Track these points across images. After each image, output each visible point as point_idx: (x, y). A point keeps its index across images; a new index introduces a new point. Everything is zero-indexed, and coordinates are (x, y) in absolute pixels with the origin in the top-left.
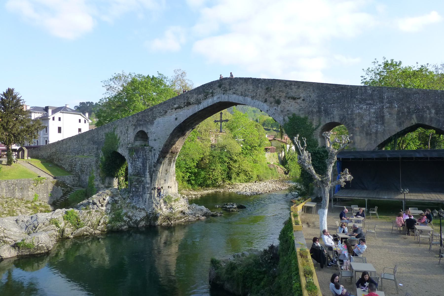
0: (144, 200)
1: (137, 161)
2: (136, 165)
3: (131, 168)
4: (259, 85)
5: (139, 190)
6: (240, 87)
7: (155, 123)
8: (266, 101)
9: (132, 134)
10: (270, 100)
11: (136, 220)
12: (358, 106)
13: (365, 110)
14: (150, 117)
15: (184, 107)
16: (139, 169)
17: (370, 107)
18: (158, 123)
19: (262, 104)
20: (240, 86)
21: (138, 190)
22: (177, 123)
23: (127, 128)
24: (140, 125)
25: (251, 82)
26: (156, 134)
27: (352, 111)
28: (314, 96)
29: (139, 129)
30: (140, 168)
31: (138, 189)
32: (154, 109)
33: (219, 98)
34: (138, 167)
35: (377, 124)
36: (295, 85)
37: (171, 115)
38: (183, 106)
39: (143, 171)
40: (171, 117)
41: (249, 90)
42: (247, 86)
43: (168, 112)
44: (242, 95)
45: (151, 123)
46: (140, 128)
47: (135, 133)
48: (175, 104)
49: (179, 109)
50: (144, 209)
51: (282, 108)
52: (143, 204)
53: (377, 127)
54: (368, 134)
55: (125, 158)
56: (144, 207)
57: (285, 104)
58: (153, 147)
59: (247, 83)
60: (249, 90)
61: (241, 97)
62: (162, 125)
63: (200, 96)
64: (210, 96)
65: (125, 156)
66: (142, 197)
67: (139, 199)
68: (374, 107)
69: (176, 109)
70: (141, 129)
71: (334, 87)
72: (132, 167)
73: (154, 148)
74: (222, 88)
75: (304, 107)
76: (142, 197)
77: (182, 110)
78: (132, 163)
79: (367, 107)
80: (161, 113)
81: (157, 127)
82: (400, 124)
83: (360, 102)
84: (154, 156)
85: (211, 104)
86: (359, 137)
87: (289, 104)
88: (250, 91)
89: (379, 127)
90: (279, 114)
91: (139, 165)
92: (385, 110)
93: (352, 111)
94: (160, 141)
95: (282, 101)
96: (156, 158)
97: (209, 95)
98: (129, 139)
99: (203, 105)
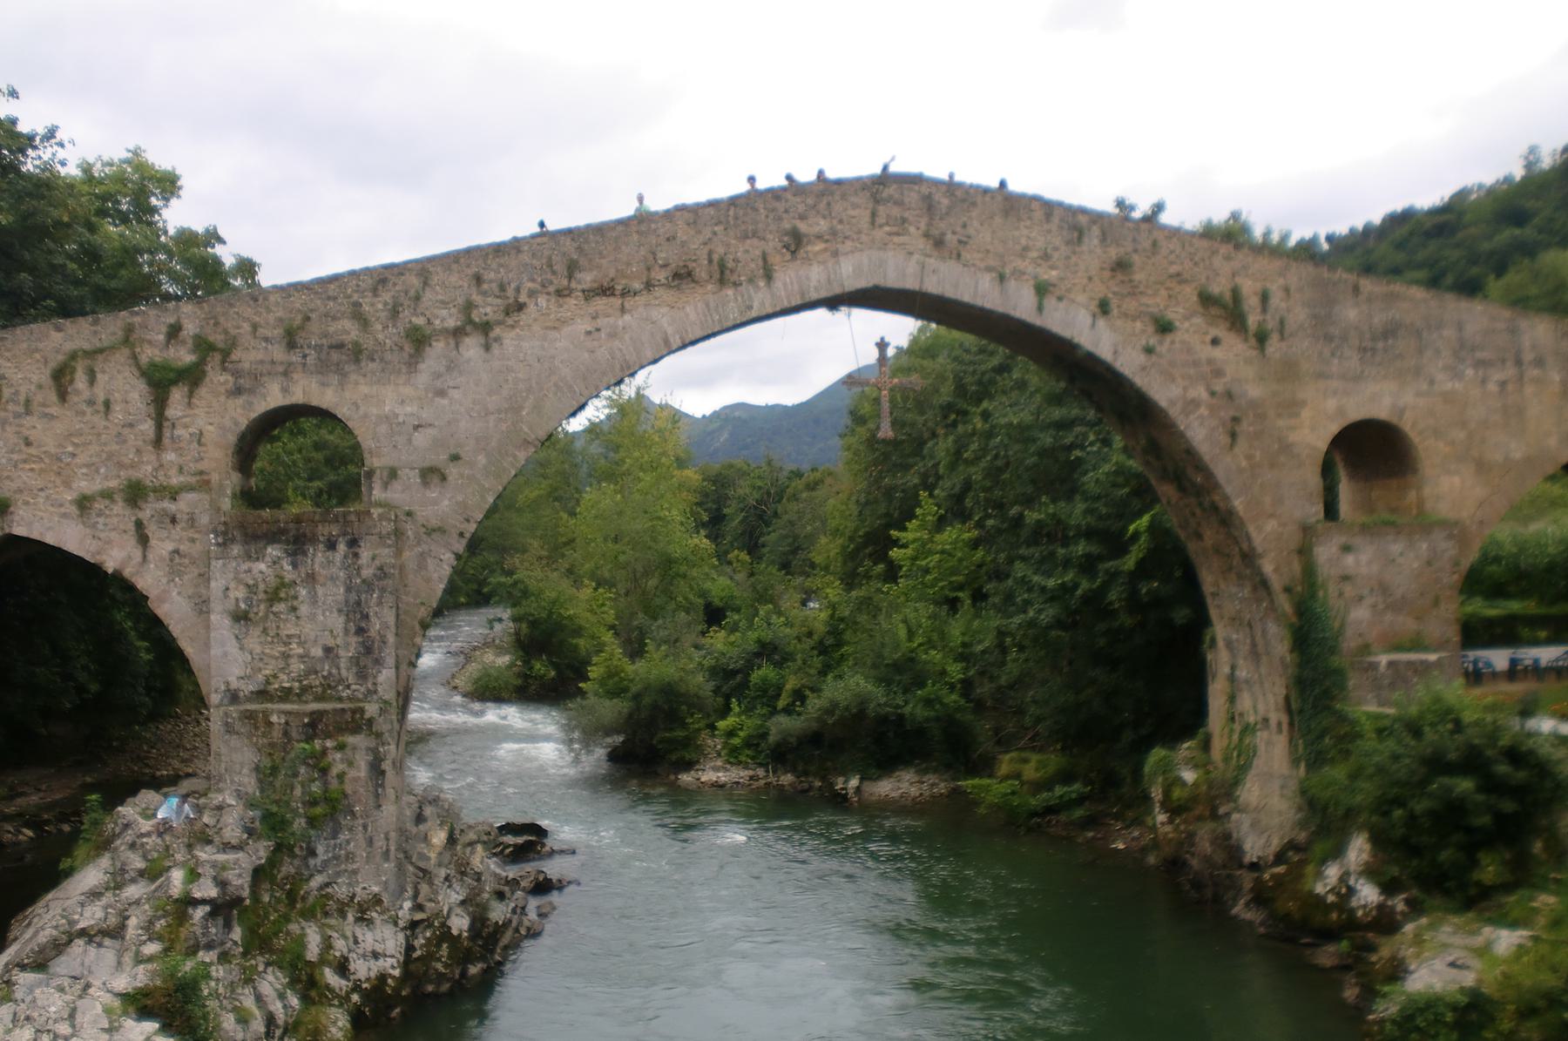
2: (292, 632)
7: (422, 366)
10: (1125, 306)
11: (382, 977)
15: (649, 286)
16: (317, 652)
18: (449, 369)
25: (1039, 214)
26: (430, 431)
27: (1432, 382)
29: (274, 397)
30: (328, 650)
37: (555, 328)
38: (637, 285)
39: (355, 661)
40: (553, 334)
41: (1026, 249)
42: (1017, 228)
43: (531, 307)
44: (989, 269)
45: (382, 360)
46: (285, 390)
47: (241, 414)
49: (616, 302)
50: (377, 900)
51: (1177, 345)
54: (1482, 467)
56: (376, 889)
57: (1187, 331)
60: (1026, 249)
63: (755, 241)
66: (365, 827)
67: (348, 842)
69: (589, 294)
70: (297, 397)
74: (887, 224)
76: (365, 827)
81: (441, 393)
84: (422, 566)
88: (1034, 254)
92: (1529, 390)
93: (1432, 382)
97: (809, 248)
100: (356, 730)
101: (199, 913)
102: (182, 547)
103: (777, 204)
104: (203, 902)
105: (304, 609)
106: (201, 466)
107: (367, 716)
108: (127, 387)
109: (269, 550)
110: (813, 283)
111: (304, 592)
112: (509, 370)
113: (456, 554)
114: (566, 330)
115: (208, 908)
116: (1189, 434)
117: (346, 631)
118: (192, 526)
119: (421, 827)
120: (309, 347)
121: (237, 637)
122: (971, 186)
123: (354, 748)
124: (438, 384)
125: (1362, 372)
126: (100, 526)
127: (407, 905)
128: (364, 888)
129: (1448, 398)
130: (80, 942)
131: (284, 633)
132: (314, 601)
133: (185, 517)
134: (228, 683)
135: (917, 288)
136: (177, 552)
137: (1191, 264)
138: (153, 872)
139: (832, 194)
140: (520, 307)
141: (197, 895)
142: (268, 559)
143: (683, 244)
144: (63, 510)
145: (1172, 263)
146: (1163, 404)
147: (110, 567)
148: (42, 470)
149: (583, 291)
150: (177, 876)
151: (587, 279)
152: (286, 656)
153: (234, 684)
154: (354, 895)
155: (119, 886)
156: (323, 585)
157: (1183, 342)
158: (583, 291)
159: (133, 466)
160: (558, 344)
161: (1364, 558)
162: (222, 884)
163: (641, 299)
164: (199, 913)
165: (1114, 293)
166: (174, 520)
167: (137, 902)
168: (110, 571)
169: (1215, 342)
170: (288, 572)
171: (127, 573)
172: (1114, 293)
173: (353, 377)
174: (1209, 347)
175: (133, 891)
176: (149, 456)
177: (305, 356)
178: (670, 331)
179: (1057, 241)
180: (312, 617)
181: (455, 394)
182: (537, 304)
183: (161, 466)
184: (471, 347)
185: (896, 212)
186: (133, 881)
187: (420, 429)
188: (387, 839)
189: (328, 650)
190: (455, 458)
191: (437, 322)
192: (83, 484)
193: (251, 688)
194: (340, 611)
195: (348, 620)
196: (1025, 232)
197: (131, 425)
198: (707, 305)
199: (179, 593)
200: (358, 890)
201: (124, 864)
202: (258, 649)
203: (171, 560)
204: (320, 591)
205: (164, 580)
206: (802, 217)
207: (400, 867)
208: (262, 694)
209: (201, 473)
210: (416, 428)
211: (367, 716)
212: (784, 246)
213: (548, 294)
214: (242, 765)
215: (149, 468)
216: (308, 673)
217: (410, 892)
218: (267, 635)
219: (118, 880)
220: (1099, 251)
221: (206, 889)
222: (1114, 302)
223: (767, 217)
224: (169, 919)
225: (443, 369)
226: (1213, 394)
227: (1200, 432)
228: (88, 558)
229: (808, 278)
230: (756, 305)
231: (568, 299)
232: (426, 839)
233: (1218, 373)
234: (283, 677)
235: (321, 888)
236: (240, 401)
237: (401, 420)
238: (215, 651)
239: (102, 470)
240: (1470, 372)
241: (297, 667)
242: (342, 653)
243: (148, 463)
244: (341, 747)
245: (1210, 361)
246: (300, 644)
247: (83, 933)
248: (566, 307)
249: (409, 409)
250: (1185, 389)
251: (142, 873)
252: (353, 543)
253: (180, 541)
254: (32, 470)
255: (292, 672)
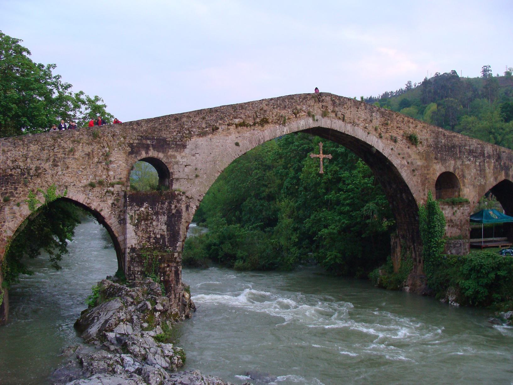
0: (177, 296)
1: (152, 219)
2: (151, 229)
3: (136, 234)
4: (374, 114)
5: (170, 279)
6: (348, 111)
7: (188, 146)
8: (381, 137)
9: (121, 162)
12: (467, 158)
13: (472, 161)
14: (175, 134)
15: (254, 124)
17: (475, 160)
18: (196, 147)
19: (376, 140)
20: (348, 110)
21: (169, 277)
22: (239, 151)
23: (107, 149)
24: (147, 148)
26: (190, 167)
28: (431, 141)
30: (161, 235)
31: (168, 276)
32: (184, 119)
33: (317, 120)
34: (156, 231)
35: (481, 177)
36: (412, 123)
37: (227, 136)
42: (357, 111)
43: (220, 130)
44: (350, 123)
45: (176, 144)
46: (147, 153)
48: (235, 118)
49: (245, 128)
50: (177, 314)
51: (399, 148)
52: (176, 305)
53: (480, 180)
55: (102, 213)
57: (401, 144)
58: (184, 193)
59: (358, 108)
60: (359, 117)
61: (349, 125)
62: (206, 151)
64: (303, 114)
65: (101, 210)
66: (174, 292)
68: (478, 161)
69: (237, 126)
71: (448, 134)
72: (140, 233)
73: (187, 195)
75: (421, 152)
76: (174, 292)
77: (250, 130)
78: (137, 225)
79: (473, 159)
80: (204, 128)
81: (194, 155)
82: (496, 178)
83: (469, 155)
85: (305, 128)
86: (468, 189)
87: (406, 145)
88: (362, 119)
89: (482, 180)
90: (397, 156)
91: (159, 228)
92: (486, 165)
94: (202, 183)
95: (398, 139)
96: (191, 214)
97: (300, 114)
98: (111, 173)
99: (290, 128)
100: (172, 261)
101: (157, 314)
102: (115, 202)
103: (292, 101)
104: (160, 311)
105: (154, 223)
106: (122, 176)
107: (175, 256)
108: (99, 150)
109: (145, 204)
110: (302, 125)
111: (155, 217)
112: (214, 149)
113: (197, 206)
114: (230, 137)
116: (402, 174)
117: (167, 231)
118: (118, 196)
120: (154, 139)
121: (135, 231)
122: (345, 98)
123: (172, 267)
124: (193, 152)
125: (446, 158)
126: (90, 195)
127: (184, 315)
128: (174, 310)
129: (468, 167)
130: (122, 323)
131: (148, 230)
132: (158, 221)
133: (117, 192)
134: (132, 246)
135: (329, 127)
136: (113, 204)
137: (403, 124)
139: (307, 98)
140: (218, 128)
141: (158, 309)
142: (144, 206)
143: (265, 111)
144: (79, 189)
145: (399, 124)
146: (395, 166)
147: (93, 207)
148: (72, 176)
149: (236, 124)
151: (237, 121)
152: (149, 238)
153: (134, 246)
155: (126, 307)
156: (161, 215)
157: (400, 147)
158: (236, 124)
159: (101, 176)
160: (228, 141)
161: (447, 212)
162: (164, 306)
163: (253, 128)
164: (157, 314)
165: (382, 132)
166: (113, 194)
168: (93, 209)
169: (409, 148)
170: (150, 211)
171: (98, 210)
172: (382, 132)
173: (167, 149)
174: (408, 149)
176: (105, 172)
177: (153, 142)
178: (260, 138)
179: (368, 116)
180: (157, 226)
181: (197, 155)
182: (222, 128)
183: (109, 176)
184: (202, 141)
185: (324, 104)
186: (130, 305)
187: (187, 166)
188: (180, 295)
189: (161, 235)
190: (197, 176)
191: (192, 133)
192: (85, 181)
193: (139, 247)
194: (166, 224)
195: (167, 227)
196: (359, 112)
197: (101, 162)
198: (271, 131)
199: (114, 217)
201: (127, 300)
202: (141, 236)
203: (112, 206)
204: (160, 217)
205: (110, 213)
206: (299, 105)
208: (143, 248)
209: (120, 179)
210: (186, 166)
211: (175, 256)
212: (293, 113)
213: (225, 125)
214: (138, 271)
215: (105, 177)
216: (156, 243)
218: (144, 231)
220: (379, 119)
222: (383, 135)
223: (289, 104)
224: (149, 316)
225: (194, 148)
226: (408, 163)
227: (405, 174)
228: (86, 205)
229: (300, 123)
230: (285, 131)
231: (231, 127)
233: (409, 156)
234: (148, 244)
236: (133, 156)
237: (181, 163)
238: (128, 236)
239: (91, 177)
240: (472, 159)
241: (152, 240)
242: (166, 236)
243: (105, 175)
244: (168, 266)
245: (408, 153)
246: (154, 234)
247: (122, 320)
248: (231, 129)
249: (183, 160)
250: (401, 161)
251: (132, 303)
252: (170, 203)
253: (115, 200)
254: (69, 176)
255: (151, 242)
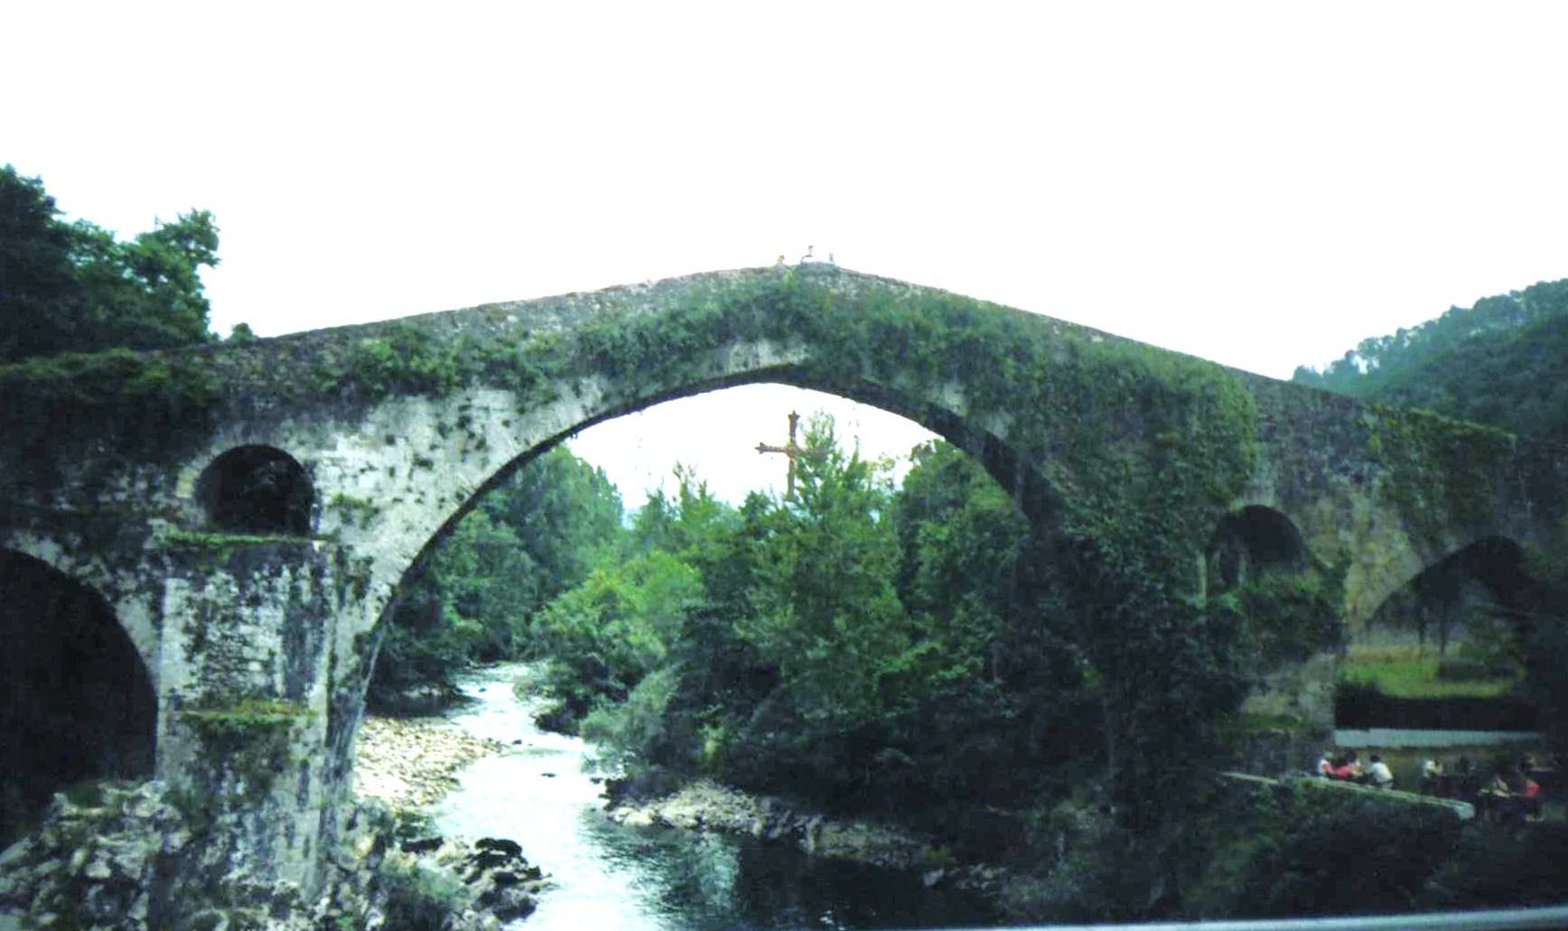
56: (294, 884)
101: (93, 892)
104: (96, 881)
111: (246, 612)
115: (101, 887)
119: (352, 833)
127: (325, 901)
138: (63, 851)
141: (91, 874)
150: (79, 857)
153: (180, 692)
154: (273, 888)
167: (47, 877)
175: (45, 868)
200: (277, 884)
207: (320, 865)
210: (363, 471)
217: (329, 889)
219: (38, 853)
221: (101, 870)
232: (353, 844)
235: (240, 879)
